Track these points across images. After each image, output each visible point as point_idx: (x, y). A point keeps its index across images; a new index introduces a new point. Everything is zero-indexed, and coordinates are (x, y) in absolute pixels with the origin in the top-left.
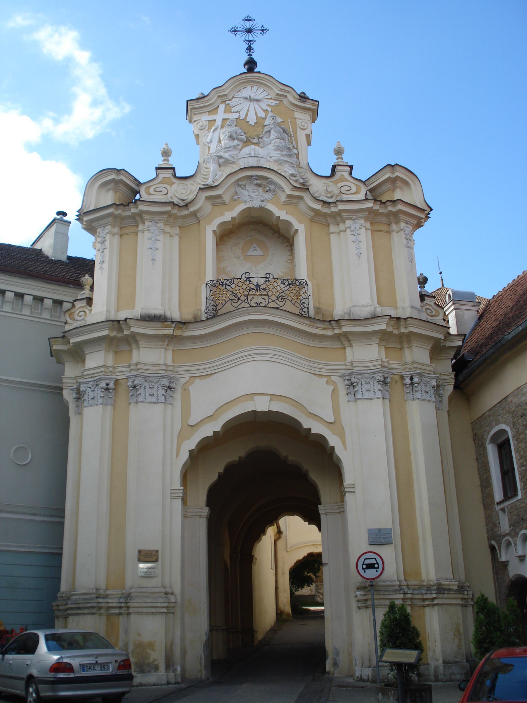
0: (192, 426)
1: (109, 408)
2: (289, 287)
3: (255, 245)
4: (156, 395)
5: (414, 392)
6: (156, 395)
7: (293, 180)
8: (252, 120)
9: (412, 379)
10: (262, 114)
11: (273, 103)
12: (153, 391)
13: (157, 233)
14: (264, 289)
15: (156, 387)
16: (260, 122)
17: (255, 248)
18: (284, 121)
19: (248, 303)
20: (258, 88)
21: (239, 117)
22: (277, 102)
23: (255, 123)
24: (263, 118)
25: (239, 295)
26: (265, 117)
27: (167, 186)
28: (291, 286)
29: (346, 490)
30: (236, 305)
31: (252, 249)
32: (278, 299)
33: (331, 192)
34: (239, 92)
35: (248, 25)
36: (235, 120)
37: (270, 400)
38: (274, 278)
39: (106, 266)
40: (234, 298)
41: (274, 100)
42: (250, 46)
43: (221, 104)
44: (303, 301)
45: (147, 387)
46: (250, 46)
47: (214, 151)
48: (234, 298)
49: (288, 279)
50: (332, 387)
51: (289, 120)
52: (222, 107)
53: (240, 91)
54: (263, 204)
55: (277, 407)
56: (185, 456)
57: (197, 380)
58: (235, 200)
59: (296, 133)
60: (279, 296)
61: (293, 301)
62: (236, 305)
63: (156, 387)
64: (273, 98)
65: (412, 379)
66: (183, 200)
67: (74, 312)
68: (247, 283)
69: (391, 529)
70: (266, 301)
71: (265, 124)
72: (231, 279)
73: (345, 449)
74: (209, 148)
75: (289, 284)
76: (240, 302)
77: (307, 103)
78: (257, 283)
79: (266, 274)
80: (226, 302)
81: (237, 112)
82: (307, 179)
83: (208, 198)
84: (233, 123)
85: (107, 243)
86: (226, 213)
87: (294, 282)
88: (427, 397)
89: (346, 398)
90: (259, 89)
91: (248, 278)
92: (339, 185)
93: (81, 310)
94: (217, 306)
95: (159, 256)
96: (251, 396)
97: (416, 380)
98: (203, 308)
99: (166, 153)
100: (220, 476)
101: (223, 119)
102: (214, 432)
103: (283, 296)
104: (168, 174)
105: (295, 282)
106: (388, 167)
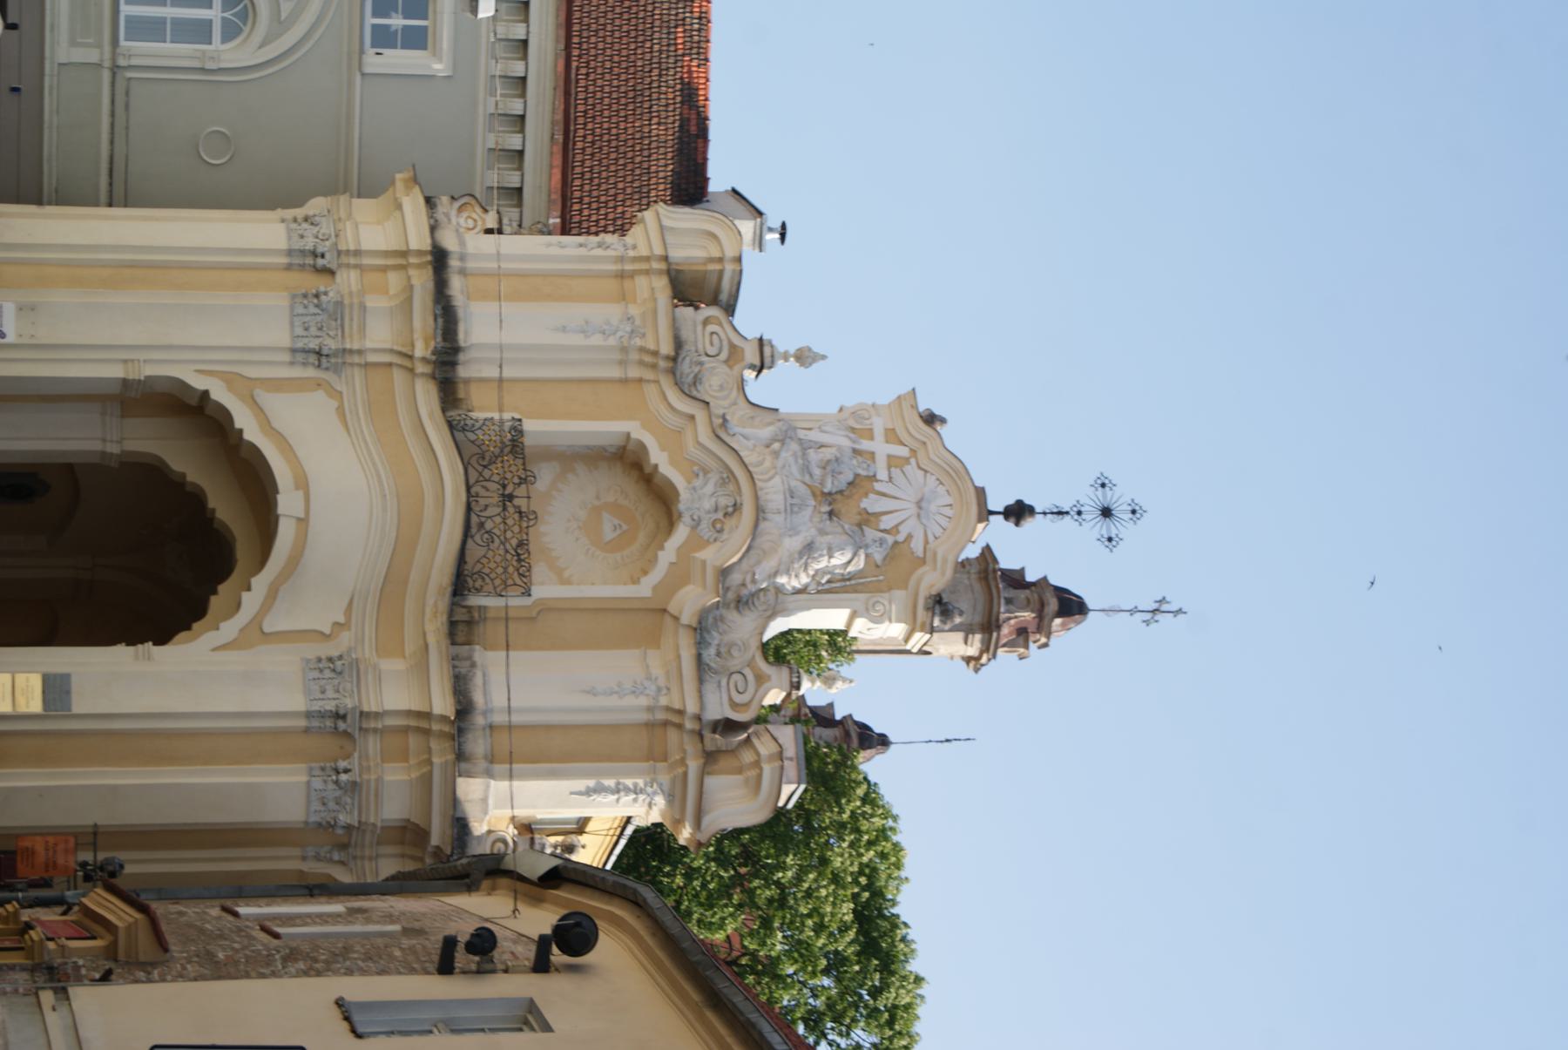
0: (252, 397)
1: (284, 260)
2: (514, 556)
3: (625, 527)
4: (305, 333)
5: (325, 778)
6: (305, 333)
7: (744, 580)
8: (872, 504)
9: (346, 771)
10: (887, 522)
11: (917, 546)
12: (313, 331)
13: (620, 334)
14: (505, 509)
15: (319, 334)
16: (867, 519)
17: (618, 527)
18: (877, 566)
19: (477, 482)
20: (950, 518)
21: (877, 481)
22: (921, 555)
23: (865, 509)
24: (878, 524)
25: (492, 467)
26: (882, 526)
27: (724, 356)
28: (516, 558)
29: (140, 646)
30: (473, 461)
31: (616, 522)
32: (487, 532)
33: (731, 655)
34: (938, 482)
35: (1121, 511)
36: (871, 474)
37: (299, 520)
38: (527, 527)
39: (555, 251)
40: (487, 458)
41: (925, 548)
42: (1067, 513)
43: (911, 449)
44: (487, 580)
45: (319, 318)
46: (1067, 513)
47: (802, 437)
48: (487, 458)
49: (529, 553)
50: (327, 631)
51: (881, 578)
52: (903, 451)
53: (941, 483)
54: (686, 519)
55: (286, 533)
56: (199, 383)
57: (335, 404)
58: (697, 471)
59: (856, 591)
60: (495, 537)
61: (484, 561)
62: (473, 461)
63: (319, 334)
64: (928, 546)
65: (346, 771)
66: (695, 384)
67: (475, 211)
68: (516, 480)
69: (70, 710)
70: (481, 511)
71: (864, 527)
72: (522, 454)
73: (214, 650)
74: (810, 429)
75: (518, 555)
76: (480, 469)
77: (925, 613)
78: (517, 497)
79: (534, 512)
80: (478, 446)
81: (890, 478)
82: (752, 608)
83: (692, 417)
84: (863, 469)
85: (599, 252)
86: (665, 455)
87: (523, 564)
88: (316, 806)
89: (311, 655)
90: (948, 520)
91: (525, 479)
92: (747, 671)
93: (480, 223)
94: (473, 432)
95: (577, 340)
96: (302, 483)
97: (344, 777)
98: (474, 415)
99: (804, 357)
100: (184, 475)
101: (873, 454)
102: (241, 431)
103: (493, 542)
104: (752, 356)
105: (524, 566)
106: (779, 749)
